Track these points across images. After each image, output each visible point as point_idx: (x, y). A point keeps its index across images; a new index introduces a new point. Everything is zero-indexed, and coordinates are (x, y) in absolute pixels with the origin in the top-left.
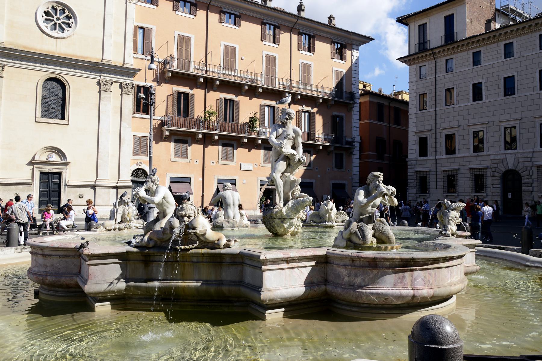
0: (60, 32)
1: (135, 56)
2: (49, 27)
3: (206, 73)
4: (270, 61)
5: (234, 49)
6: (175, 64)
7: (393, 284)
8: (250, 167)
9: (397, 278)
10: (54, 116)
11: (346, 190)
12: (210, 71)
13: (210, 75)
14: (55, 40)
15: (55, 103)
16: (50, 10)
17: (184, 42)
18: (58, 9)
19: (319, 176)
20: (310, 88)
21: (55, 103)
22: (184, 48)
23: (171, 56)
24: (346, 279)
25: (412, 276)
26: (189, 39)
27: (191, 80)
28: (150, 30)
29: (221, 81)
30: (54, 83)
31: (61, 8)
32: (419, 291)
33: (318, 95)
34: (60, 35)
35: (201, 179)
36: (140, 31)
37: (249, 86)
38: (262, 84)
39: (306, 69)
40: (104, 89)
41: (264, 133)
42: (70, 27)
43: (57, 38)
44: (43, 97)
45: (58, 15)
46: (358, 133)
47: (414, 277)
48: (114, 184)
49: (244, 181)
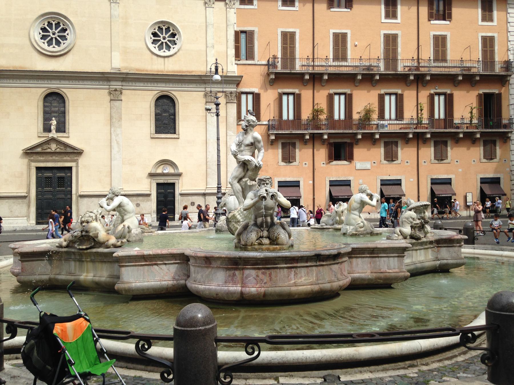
0: (167, 51)
1: (239, 62)
2: (157, 48)
4: (391, 41)
6: (279, 65)
7: (224, 281)
8: (368, 165)
9: (228, 275)
10: (167, 131)
11: (502, 186)
12: (318, 66)
13: (317, 70)
14: (162, 59)
16: (156, 31)
17: (288, 39)
18: (164, 28)
19: (460, 170)
20: (445, 64)
22: (288, 46)
23: (275, 57)
24: (193, 275)
25: (243, 274)
27: (297, 78)
29: (329, 74)
30: (165, 100)
31: (166, 27)
32: (247, 289)
33: (454, 71)
36: (243, 36)
39: (440, 42)
40: (210, 101)
41: (383, 126)
42: (176, 44)
43: (164, 57)
44: (156, 115)
47: (245, 275)
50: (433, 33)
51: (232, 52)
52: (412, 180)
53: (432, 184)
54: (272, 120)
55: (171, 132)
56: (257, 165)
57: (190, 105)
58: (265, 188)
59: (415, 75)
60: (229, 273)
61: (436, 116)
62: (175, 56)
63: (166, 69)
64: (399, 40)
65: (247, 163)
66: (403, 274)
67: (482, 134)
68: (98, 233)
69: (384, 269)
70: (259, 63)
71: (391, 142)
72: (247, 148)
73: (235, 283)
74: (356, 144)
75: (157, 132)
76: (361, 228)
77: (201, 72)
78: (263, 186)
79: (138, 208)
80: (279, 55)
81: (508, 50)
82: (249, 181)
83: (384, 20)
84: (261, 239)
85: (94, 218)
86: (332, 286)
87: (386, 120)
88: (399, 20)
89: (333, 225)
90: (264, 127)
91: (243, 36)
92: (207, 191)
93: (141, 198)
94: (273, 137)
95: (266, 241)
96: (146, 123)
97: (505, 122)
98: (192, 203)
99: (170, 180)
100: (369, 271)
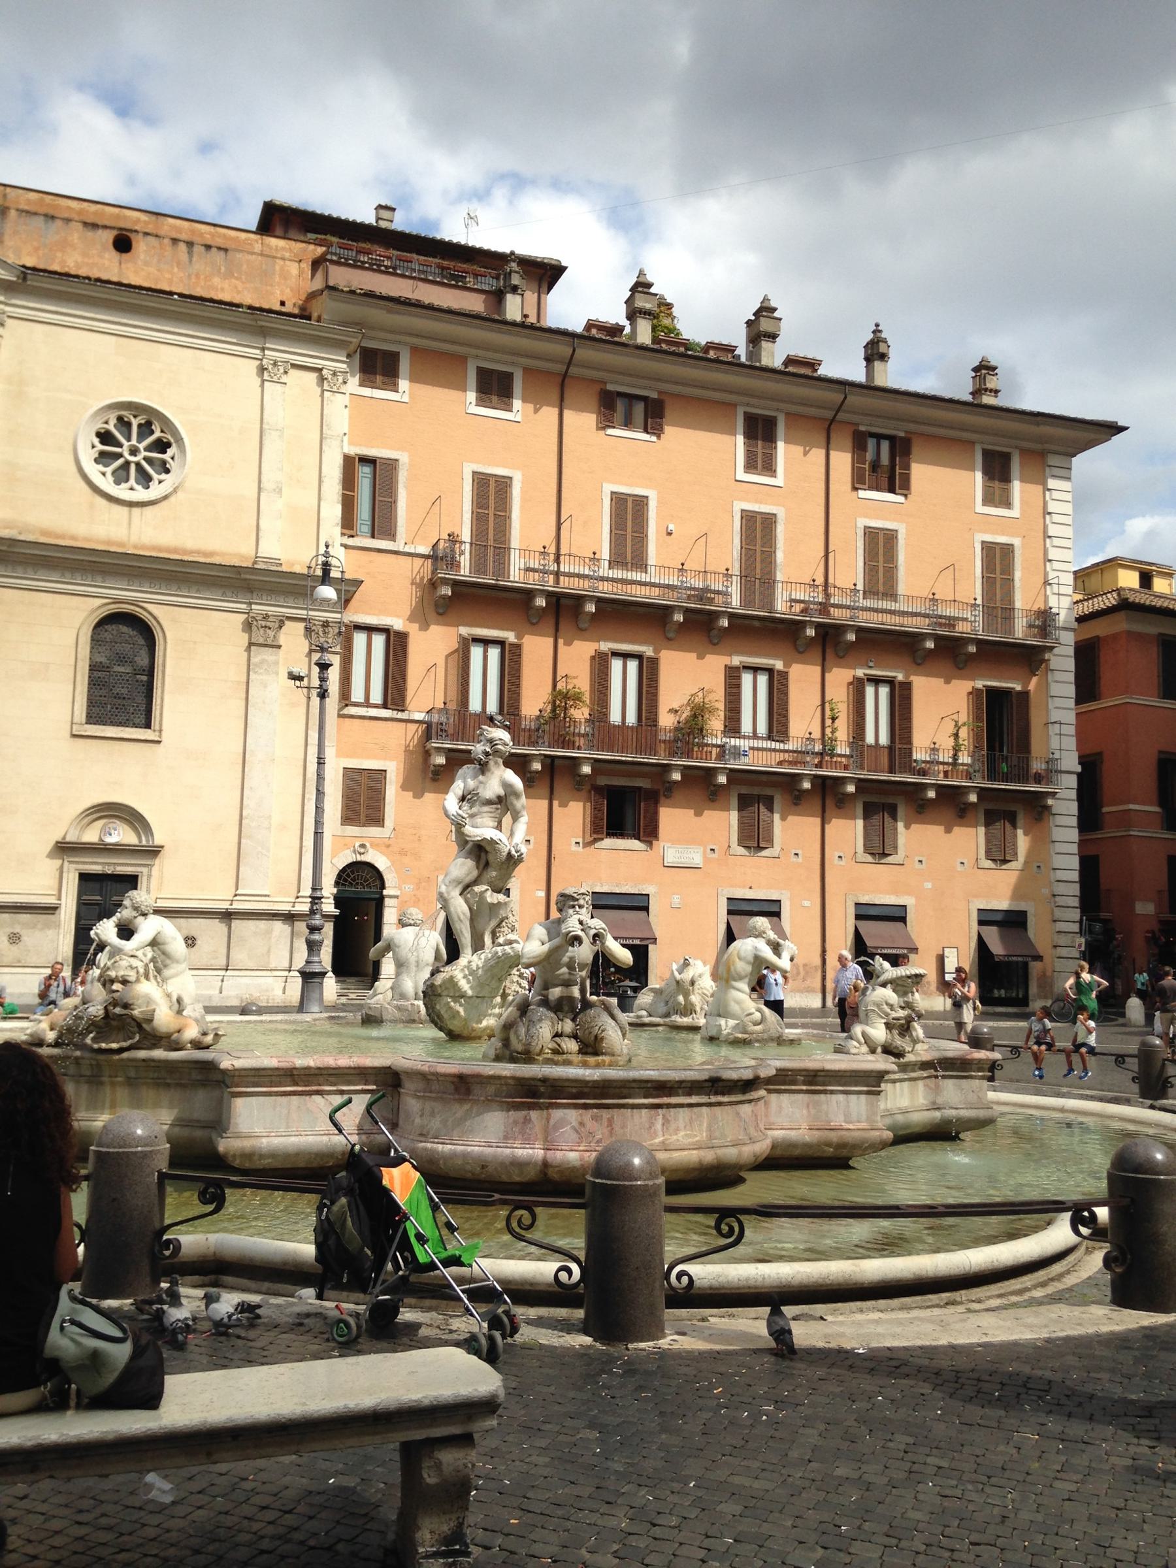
0: (139, 487)
2: (109, 475)
3: (557, 582)
4: (758, 530)
5: (641, 503)
6: (465, 561)
7: (501, 1135)
8: (695, 857)
9: (511, 1121)
10: (123, 718)
12: (570, 575)
13: (568, 585)
14: (124, 510)
15: (122, 685)
16: (111, 427)
17: (491, 494)
18: (135, 423)
19: (928, 885)
21: (122, 685)
22: (491, 512)
23: (453, 539)
24: (418, 1121)
25: (548, 1120)
26: (504, 484)
27: (512, 603)
28: (391, 466)
29: (600, 601)
30: (124, 629)
31: (141, 419)
32: (559, 1154)
34: (140, 494)
35: (542, 894)
36: (364, 474)
37: (687, 611)
38: (727, 604)
39: (881, 546)
40: (261, 641)
41: (737, 753)
42: (167, 471)
43: (131, 504)
44: (93, 668)
45: (134, 442)
46: (1071, 743)
47: (552, 1122)
48: (285, 908)
49: (676, 899)
50: (862, 522)
51: (333, 511)
52: (807, 903)
53: (858, 917)
54: (440, 711)
55: (137, 721)
56: (513, 852)
57: (197, 645)
58: (577, 917)
59: (819, 626)
60: (514, 1115)
61: (870, 739)
62: (164, 503)
63: (134, 539)
64: (780, 530)
65: (488, 848)
66: (877, 1133)
67: (982, 792)
68: (154, 1011)
69: (838, 1120)
70: (407, 550)
71: (758, 797)
72: (486, 809)
73: (528, 1141)
74: (667, 797)
75: (91, 719)
76: (756, 1024)
77: (242, 557)
78: (571, 911)
79: (14, 948)
80: (466, 535)
81: (1046, 583)
82: (489, 893)
83: (741, 475)
84: (557, 1039)
85: (142, 971)
86: (740, 1153)
87: (744, 737)
88: (779, 481)
89: (667, 1015)
90: (414, 727)
91: (364, 474)
92: (237, 906)
93: (25, 917)
94: (441, 760)
95: (571, 1046)
96: (62, 692)
97: (1037, 766)
98: (193, 939)
99: (124, 867)
100: (805, 1126)
